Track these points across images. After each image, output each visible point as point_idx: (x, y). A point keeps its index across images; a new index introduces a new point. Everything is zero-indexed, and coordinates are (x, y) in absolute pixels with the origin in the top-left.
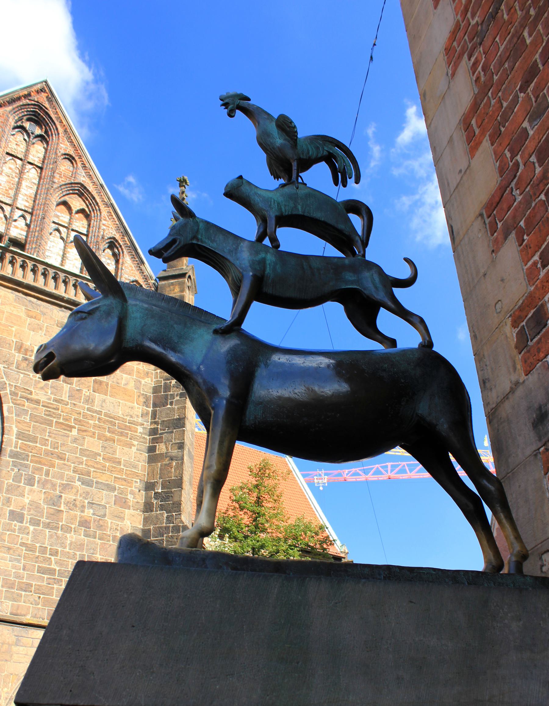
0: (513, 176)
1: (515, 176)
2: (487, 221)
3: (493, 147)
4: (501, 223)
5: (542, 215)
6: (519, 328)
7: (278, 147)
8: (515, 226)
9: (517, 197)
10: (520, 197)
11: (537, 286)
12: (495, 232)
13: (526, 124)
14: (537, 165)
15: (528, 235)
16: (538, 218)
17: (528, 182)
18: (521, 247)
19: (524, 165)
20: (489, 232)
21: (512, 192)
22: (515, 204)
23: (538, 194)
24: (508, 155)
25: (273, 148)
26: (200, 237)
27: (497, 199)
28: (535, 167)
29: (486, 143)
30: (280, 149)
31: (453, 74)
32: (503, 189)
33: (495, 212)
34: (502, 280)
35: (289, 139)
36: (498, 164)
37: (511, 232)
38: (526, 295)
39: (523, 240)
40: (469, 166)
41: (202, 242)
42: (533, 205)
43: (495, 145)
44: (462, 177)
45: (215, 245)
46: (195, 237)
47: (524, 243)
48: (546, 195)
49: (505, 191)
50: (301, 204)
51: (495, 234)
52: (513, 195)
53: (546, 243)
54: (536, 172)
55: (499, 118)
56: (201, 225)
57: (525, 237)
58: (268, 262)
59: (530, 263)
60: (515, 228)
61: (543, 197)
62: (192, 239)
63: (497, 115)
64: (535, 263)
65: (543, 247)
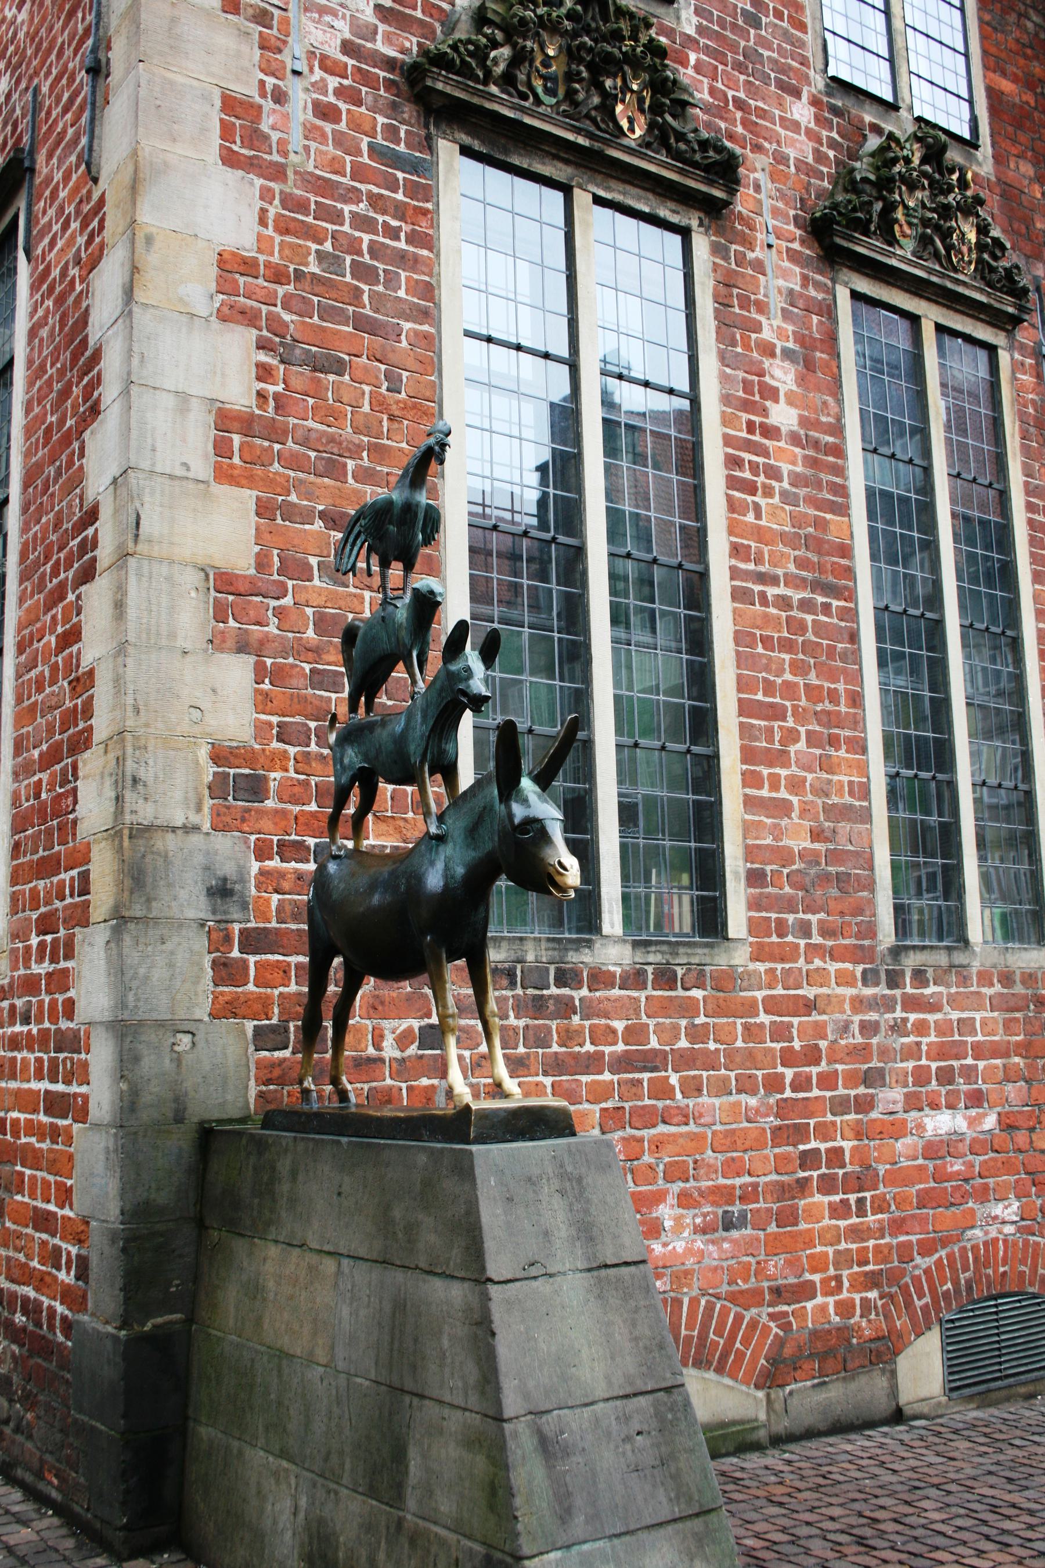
1: (278, 598)
4: (238, 625)
6: (220, 770)
11: (264, 750)
14: (311, 626)
16: (294, 682)
20: (211, 610)
22: (266, 629)
27: (242, 590)
31: (223, 318)
33: (231, 598)
34: (214, 691)
36: (257, 548)
42: (291, 660)
55: (280, 498)
57: (267, 681)
61: (307, 667)
63: (279, 490)
64: (270, 724)
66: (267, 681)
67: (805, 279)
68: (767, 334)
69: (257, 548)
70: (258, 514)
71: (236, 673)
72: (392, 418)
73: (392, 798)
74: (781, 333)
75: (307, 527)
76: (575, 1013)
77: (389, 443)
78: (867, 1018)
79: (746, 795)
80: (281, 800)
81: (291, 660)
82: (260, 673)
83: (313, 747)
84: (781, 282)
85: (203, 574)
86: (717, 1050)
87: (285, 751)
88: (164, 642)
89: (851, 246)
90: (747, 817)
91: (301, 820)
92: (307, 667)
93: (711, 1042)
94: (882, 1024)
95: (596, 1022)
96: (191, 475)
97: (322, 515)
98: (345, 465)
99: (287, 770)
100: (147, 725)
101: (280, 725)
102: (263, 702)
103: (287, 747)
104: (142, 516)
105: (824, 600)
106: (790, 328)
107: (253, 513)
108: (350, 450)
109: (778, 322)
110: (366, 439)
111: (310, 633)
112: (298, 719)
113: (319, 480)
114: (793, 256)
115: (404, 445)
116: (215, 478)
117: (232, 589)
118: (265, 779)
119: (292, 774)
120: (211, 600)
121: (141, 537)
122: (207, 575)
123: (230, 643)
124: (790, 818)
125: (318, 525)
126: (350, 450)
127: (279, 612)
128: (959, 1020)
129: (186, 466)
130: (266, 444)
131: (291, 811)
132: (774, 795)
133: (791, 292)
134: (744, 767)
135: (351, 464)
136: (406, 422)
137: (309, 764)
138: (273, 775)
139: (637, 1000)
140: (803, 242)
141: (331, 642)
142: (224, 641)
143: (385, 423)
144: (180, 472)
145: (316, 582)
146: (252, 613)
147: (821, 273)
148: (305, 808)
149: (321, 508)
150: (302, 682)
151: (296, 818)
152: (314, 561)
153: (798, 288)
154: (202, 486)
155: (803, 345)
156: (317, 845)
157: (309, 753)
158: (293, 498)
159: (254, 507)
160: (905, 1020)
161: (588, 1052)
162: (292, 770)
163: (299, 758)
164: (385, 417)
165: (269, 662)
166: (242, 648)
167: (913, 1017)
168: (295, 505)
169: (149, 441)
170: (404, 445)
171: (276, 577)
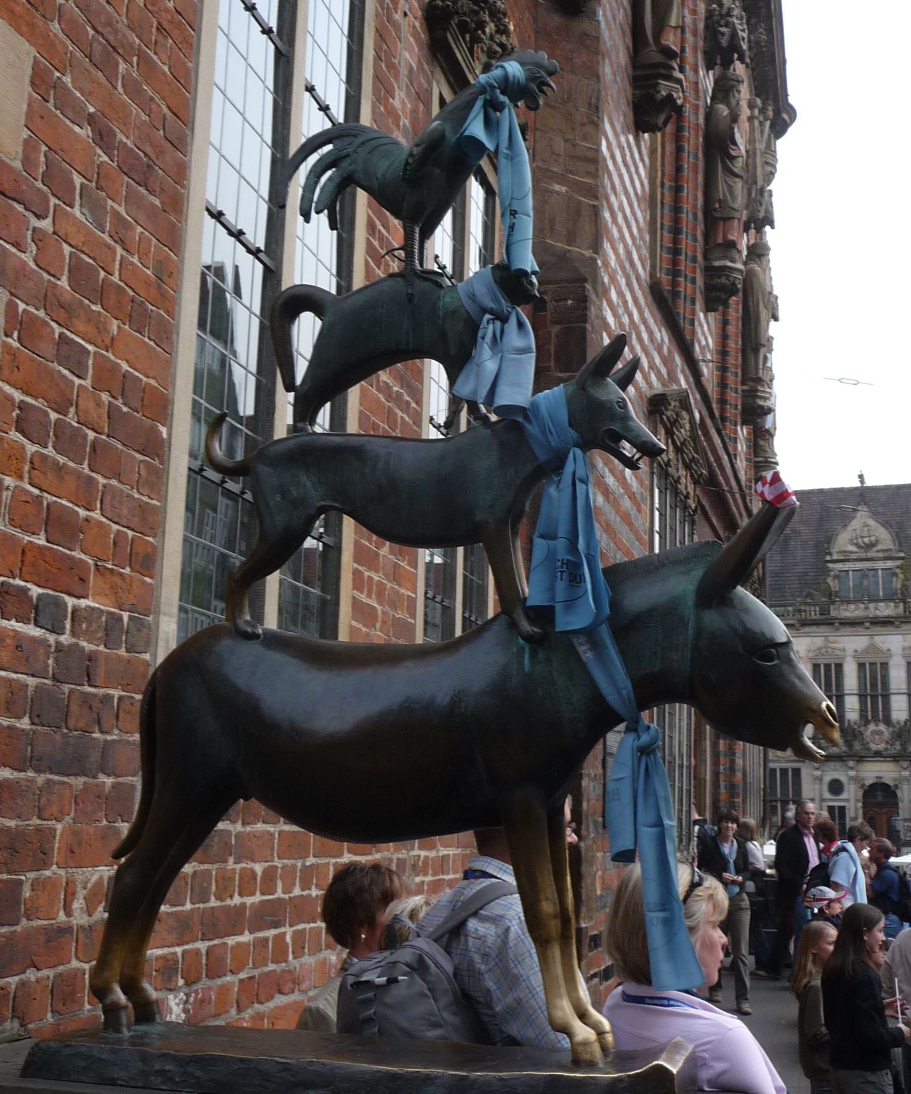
0: (38, 213)
3: (30, 89)
5: (48, 356)
8: (13, 290)
15: (20, 340)
18: (5, 339)
22: (23, 256)
36: (26, 134)
42: (41, 313)
47: (9, 340)
63: (56, 62)
66: (15, 335)
67: (419, 62)
68: (396, 103)
69: (26, 134)
70: (33, 83)
72: (160, 28)
73: (115, 543)
74: (404, 108)
75: (77, 129)
76: (231, 855)
77: (155, 57)
78: (400, 856)
79: (354, 598)
81: (41, 313)
84: (407, 55)
86: (317, 896)
87: (23, 447)
89: (454, 46)
90: (354, 623)
91: (29, 558)
92: (57, 329)
93: (313, 887)
94: (408, 862)
95: (244, 865)
97: (91, 120)
98: (117, 65)
101: (22, 406)
103: (25, 441)
105: (408, 398)
106: (409, 106)
107: (27, 80)
108: (123, 46)
109: (403, 95)
110: (137, 41)
113: (93, 71)
114: (415, 34)
115: (166, 68)
124: (375, 629)
125: (84, 132)
126: (123, 46)
127: (38, 236)
128: (443, 856)
132: (369, 601)
133: (411, 68)
134: (356, 565)
135: (122, 66)
136: (170, 41)
139: (272, 835)
140: (421, 24)
141: (81, 302)
143: (154, 30)
147: (427, 64)
148: (33, 539)
149: (92, 110)
150: (48, 349)
151: (23, 552)
152: (78, 180)
153: (415, 68)
155: (413, 129)
156: (40, 597)
158: (67, 79)
159: (29, 71)
160: (419, 856)
161: (235, 905)
163: (37, 465)
164: (155, 24)
165: (22, 306)
167: (423, 853)
168: (69, 89)
170: (166, 68)
171: (39, 184)
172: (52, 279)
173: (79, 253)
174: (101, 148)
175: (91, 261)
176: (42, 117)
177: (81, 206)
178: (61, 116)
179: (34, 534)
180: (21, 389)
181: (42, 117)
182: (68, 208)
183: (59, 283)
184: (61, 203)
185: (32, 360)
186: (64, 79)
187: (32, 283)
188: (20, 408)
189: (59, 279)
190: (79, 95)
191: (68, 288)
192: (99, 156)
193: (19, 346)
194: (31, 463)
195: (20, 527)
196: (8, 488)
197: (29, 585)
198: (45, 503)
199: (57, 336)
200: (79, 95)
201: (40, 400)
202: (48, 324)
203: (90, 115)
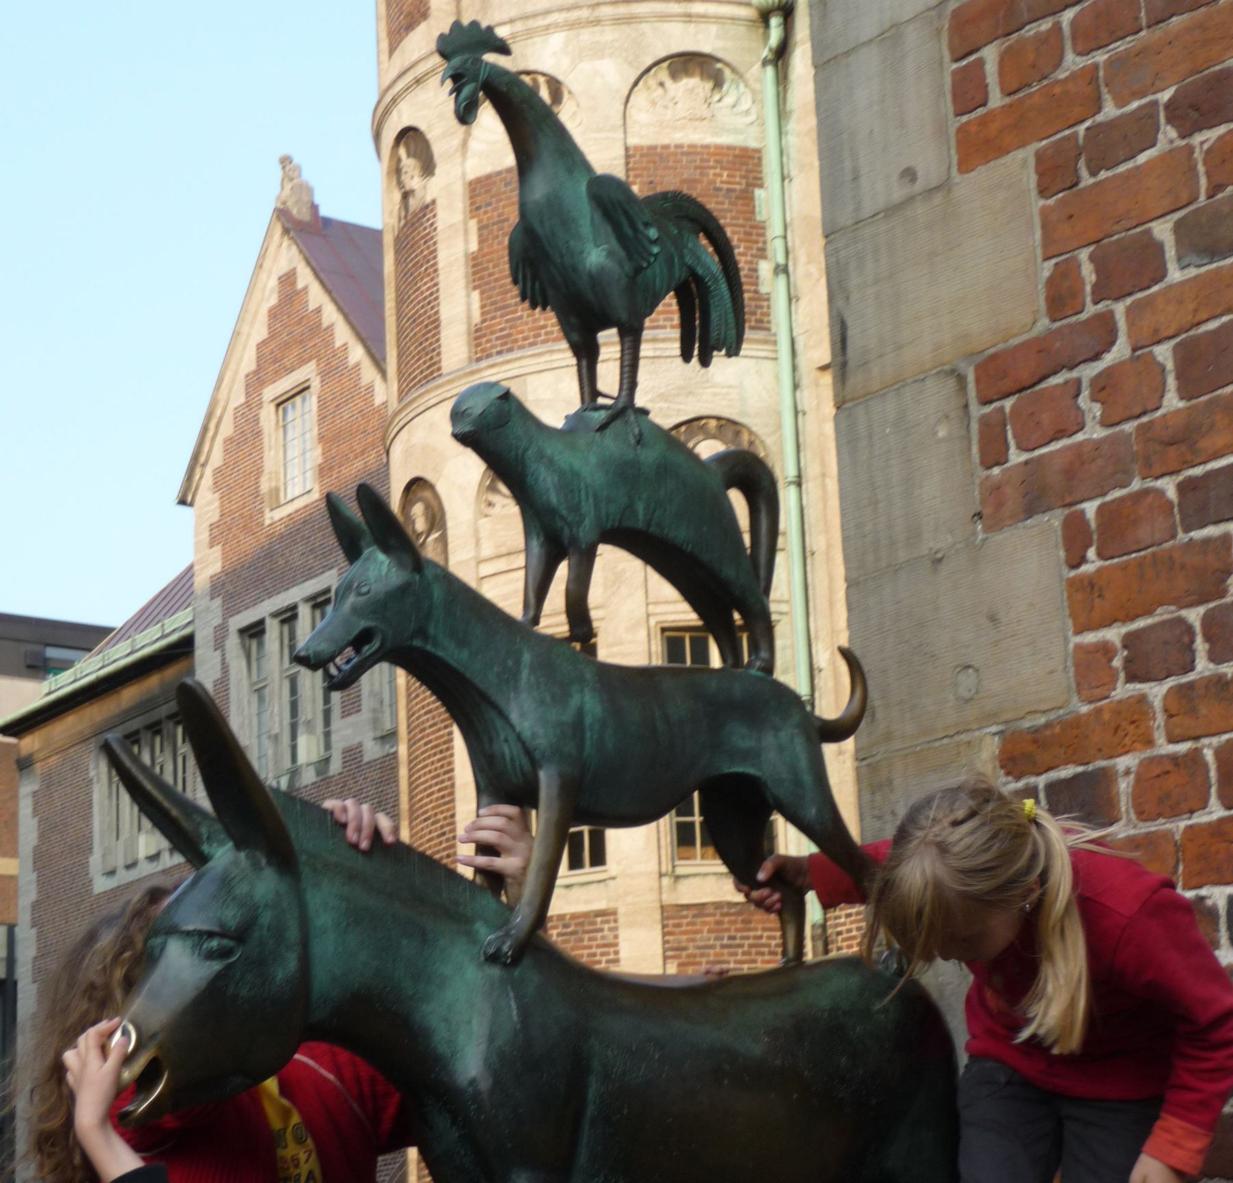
0: (1092, 354)
1: (1096, 357)
2: (977, 411)
3: (1042, 202)
4: (1025, 456)
5: (1158, 536)
7: (590, 275)
8: (1068, 500)
9: (1089, 424)
10: (1099, 433)
11: (1098, 711)
12: (997, 464)
13: (1163, 230)
14: (1171, 382)
15: (1101, 555)
17: (1138, 410)
18: (1073, 573)
19: (1134, 350)
20: (975, 449)
21: (1077, 395)
22: (1080, 437)
23: (1158, 470)
24: (1088, 273)
25: (575, 269)
26: (432, 630)
27: (1025, 377)
28: (1164, 383)
29: (1020, 165)
30: (596, 280)
32: (1048, 357)
33: (1008, 404)
34: (993, 619)
35: (623, 254)
36: (1047, 269)
37: (1049, 509)
38: (1061, 712)
39: (1083, 560)
40: (944, 186)
41: (435, 644)
42: (1136, 485)
43: (1051, 202)
44: (911, 199)
45: (465, 654)
46: (421, 632)
47: (1085, 568)
48: (1182, 488)
49: (1055, 373)
50: (644, 496)
51: (996, 471)
52: (1078, 408)
53: (1149, 621)
54: (1165, 402)
56: (437, 592)
57: (1091, 553)
58: (588, 720)
59: (1090, 638)
60: (1064, 506)
61: (1169, 487)
62: (412, 637)
64: (1106, 650)
65: (1141, 623)
70: (1043, 192)
71: (1030, 561)
75: (1142, 158)
80: (1143, 815)
82: (1076, 539)
83: (1203, 666)
85: (952, 382)
87: (1142, 699)
88: (902, 555)
92: (1169, 487)
96: (919, 186)
99: (1150, 743)
100: (888, 737)
101: (1130, 641)
102: (1088, 604)
104: (850, 322)
107: (1034, 193)
111: (1172, 401)
112: (1163, 614)
113: (1159, 32)
116: (960, 163)
117: (1008, 384)
118: (1105, 778)
119: (1165, 748)
120: (975, 427)
121: (852, 363)
122: (961, 380)
123: (1013, 499)
129: (909, 174)
130: (1045, 25)
131: (1168, 835)
137: (1193, 711)
138: (1124, 762)
142: (1000, 505)
144: (898, 194)
145: (1175, 275)
146: (1046, 418)
148: (1200, 818)
149: (1165, 96)
152: (1163, 230)
154: (938, 199)
157: (1191, 686)
162: (1160, 738)
165: (1090, 508)
166: (1035, 496)
169: (847, 164)
172: (1145, 419)
173: (1192, 333)
174: (1200, 130)
175: (1225, 319)
176: (1071, 216)
177: (1179, 259)
178: (1110, 173)
179: (1192, 812)
180: (1115, 621)
181: (1071, 216)
182: (1155, 289)
183: (1159, 413)
184: (1139, 295)
185: (1124, 567)
186: (1100, 118)
187: (1100, 462)
188: (1125, 647)
189: (1157, 409)
190: (1135, 105)
191: (1181, 404)
192: (1202, 143)
193: (1099, 563)
194: (1166, 710)
195: (1159, 815)
196: (1127, 772)
197: (1204, 892)
198: (1209, 755)
199: (1172, 494)
200: (1135, 105)
201: (1159, 611)
202: (1145, 492)
203: (1169, 106)
